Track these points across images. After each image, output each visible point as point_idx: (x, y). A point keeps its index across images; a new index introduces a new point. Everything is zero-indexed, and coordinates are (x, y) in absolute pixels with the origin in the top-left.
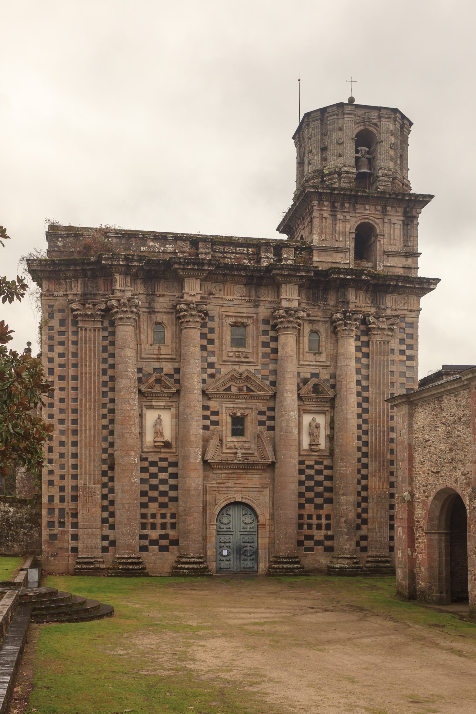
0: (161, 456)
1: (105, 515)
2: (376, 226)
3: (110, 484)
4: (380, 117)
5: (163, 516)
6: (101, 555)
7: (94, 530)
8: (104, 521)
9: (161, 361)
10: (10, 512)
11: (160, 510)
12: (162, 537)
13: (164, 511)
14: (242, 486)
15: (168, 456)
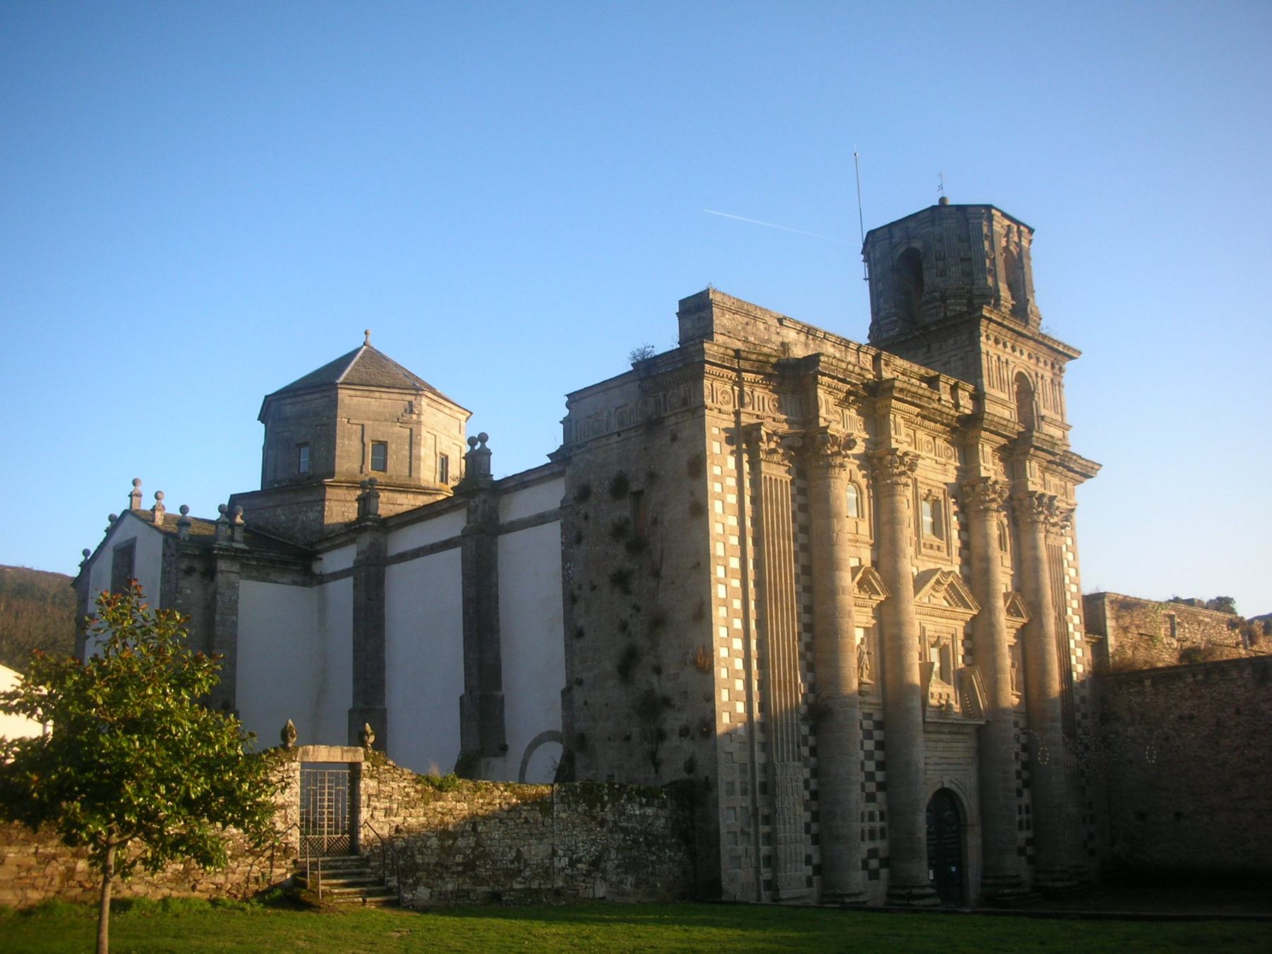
0: (866, 711)
1: (807, 816)
2: (1030, 379)
3: (813, 760)
4: (1020, 233)
5: (872, 817)
6: (805, 891)
7: (798, 845)
8: (808, 828)
9: (857, 544)
10: (649, 816)
11: (868, 806)
12: (872, 853)
13: (873, 807)
14: (951, 761)
15: (871, 711)
